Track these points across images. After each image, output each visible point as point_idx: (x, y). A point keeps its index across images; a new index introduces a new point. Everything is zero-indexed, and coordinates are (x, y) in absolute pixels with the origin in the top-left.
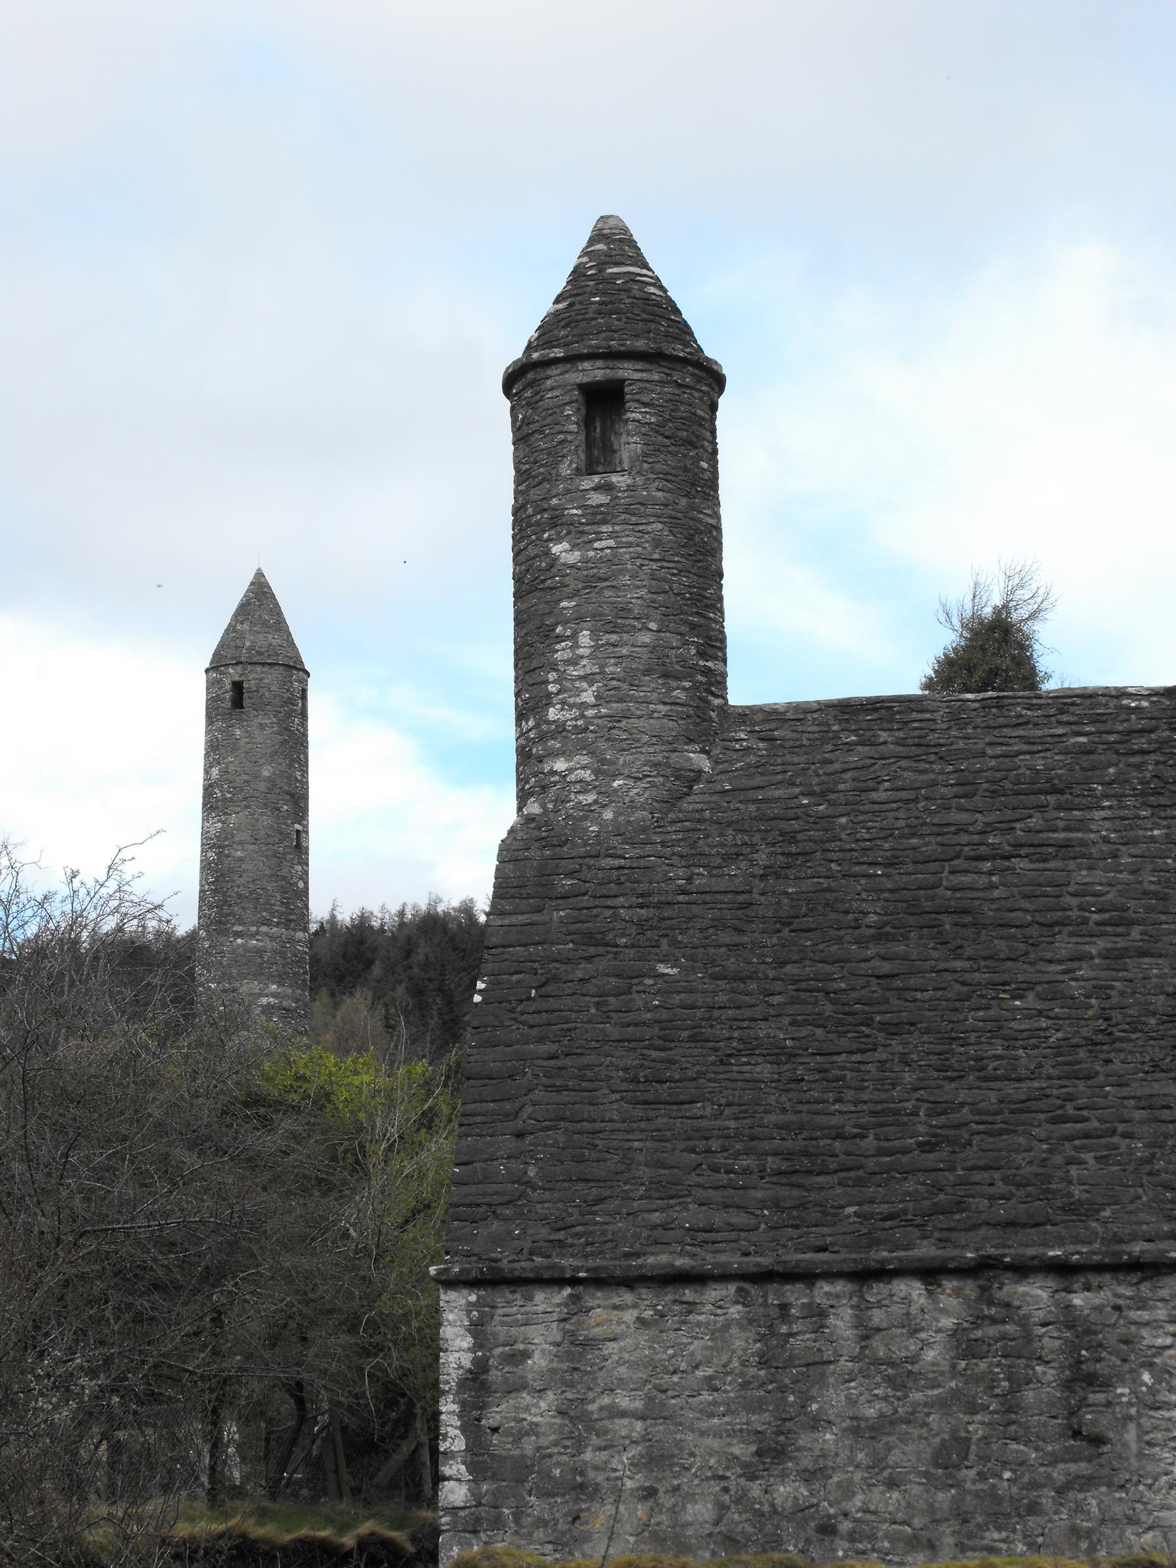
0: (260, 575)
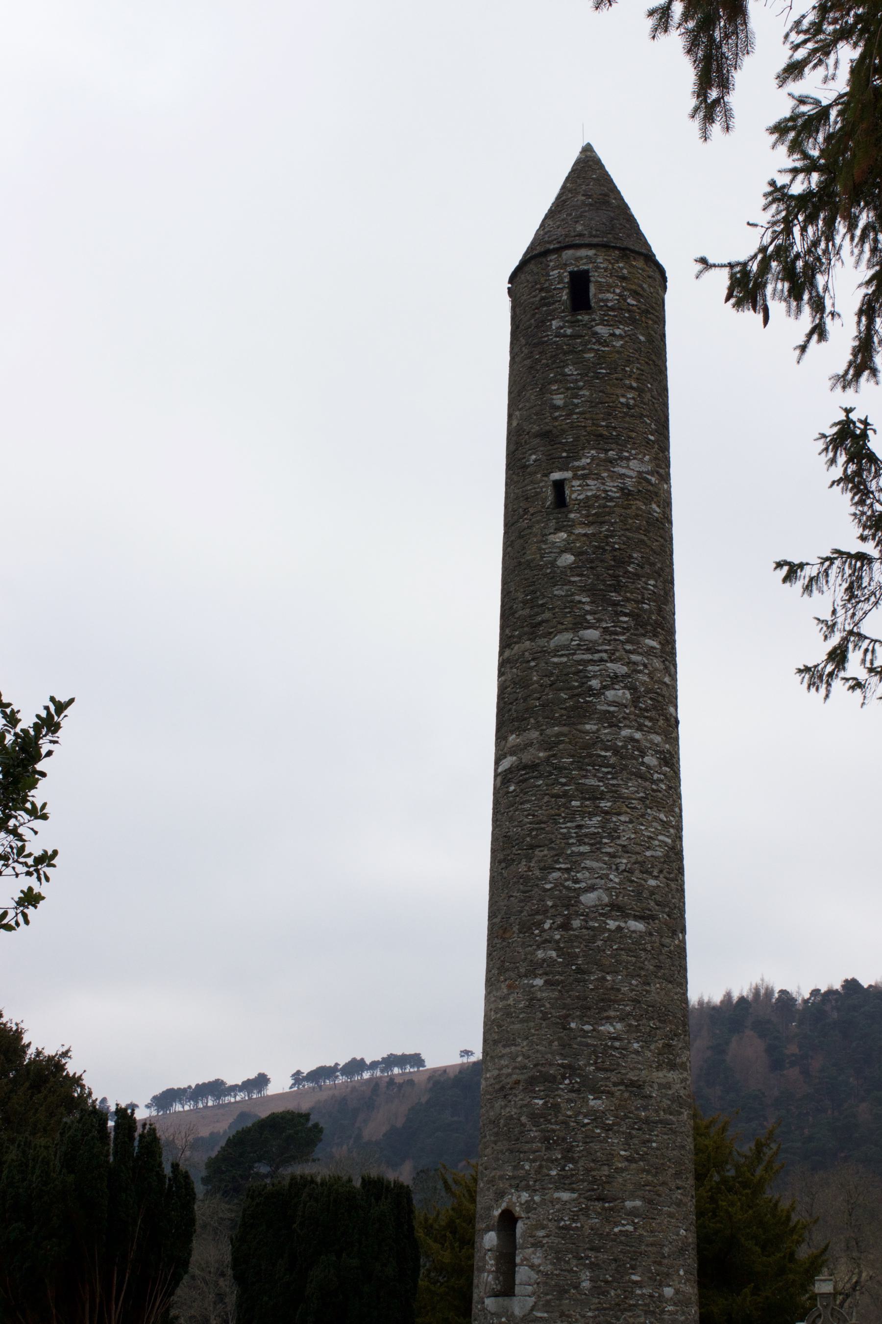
0: (588, 150)
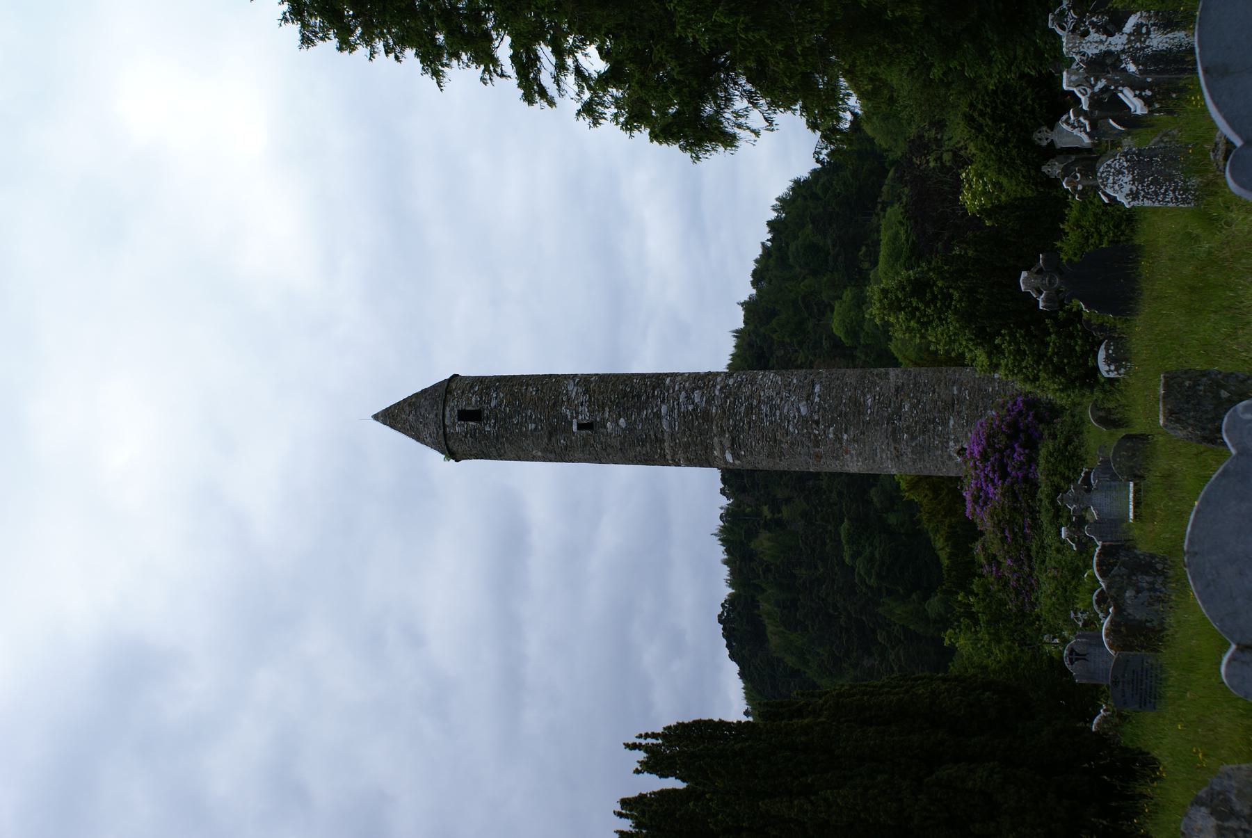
0: (376, 417)
